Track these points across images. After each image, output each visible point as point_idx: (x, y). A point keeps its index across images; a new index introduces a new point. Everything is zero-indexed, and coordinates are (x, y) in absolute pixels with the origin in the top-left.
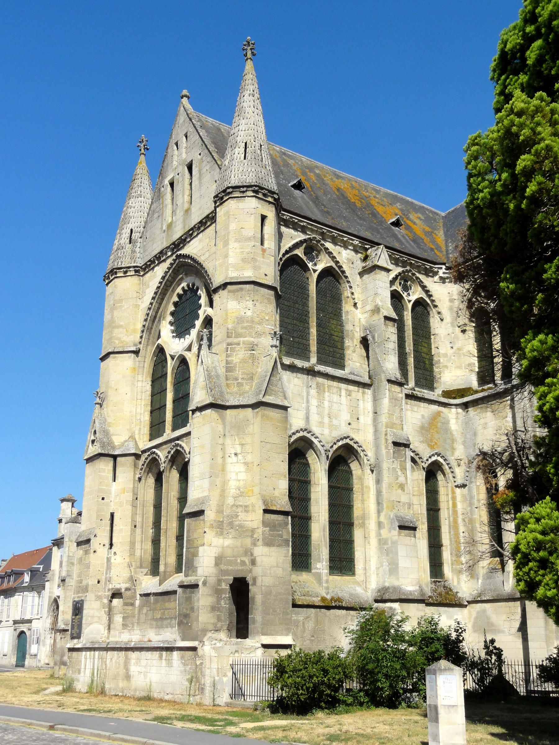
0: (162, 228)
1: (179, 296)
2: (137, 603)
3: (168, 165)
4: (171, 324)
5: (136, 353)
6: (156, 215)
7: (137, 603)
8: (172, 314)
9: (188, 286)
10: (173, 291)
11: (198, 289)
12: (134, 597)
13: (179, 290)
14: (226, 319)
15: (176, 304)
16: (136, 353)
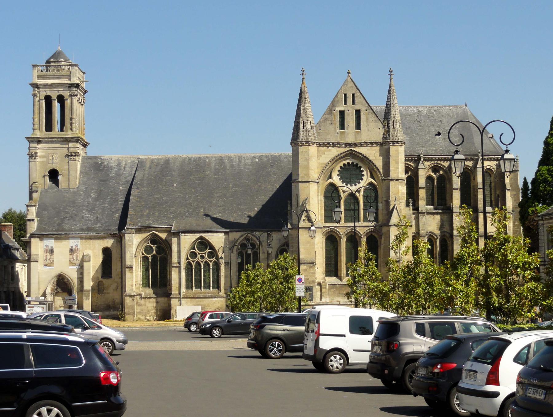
0: (336, 131)
1: (344, 164)
2: (327, 287)
3: (338, 101)
4: (338, 175)
5: (318, 183)
6: (328, 122)
7: (327, 287)
8: (339, 171)
9: (353, 163)
10: (341, 161)
11: (360, 167)
12: (326, 285)
13: (346, 162)
14: (398, 193)
15: (341, 167)
16: (318, 183)
